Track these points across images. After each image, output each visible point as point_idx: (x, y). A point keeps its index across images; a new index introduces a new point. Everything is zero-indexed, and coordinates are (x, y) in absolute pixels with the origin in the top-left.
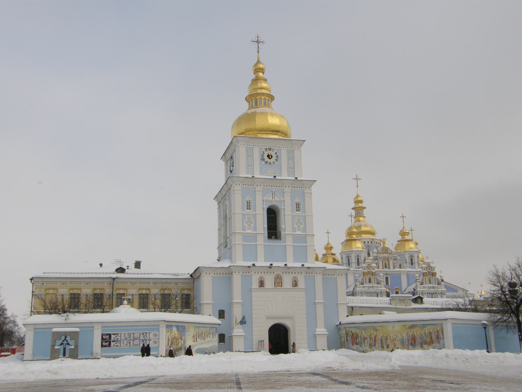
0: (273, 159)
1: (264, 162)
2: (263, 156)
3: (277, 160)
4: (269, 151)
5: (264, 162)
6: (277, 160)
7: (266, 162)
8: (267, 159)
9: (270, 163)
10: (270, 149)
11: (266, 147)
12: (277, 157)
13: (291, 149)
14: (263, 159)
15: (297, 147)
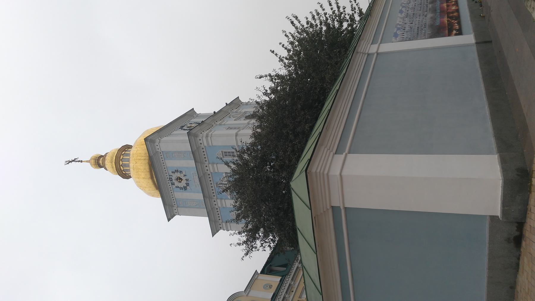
0: (181, 176)
1: (188, 187)
2: (181, 188)
3: (181, 172)
4: (174, 181)
5: (188, 187)
6: (181, 172)
7: (188, 184)
8: (183, 184)
9: (187, 180)
10: (171, 179)
11: (170, 184)
12: (177, 171)
13: (162, 154)
14: (185, 188)
15: (157, 147)
